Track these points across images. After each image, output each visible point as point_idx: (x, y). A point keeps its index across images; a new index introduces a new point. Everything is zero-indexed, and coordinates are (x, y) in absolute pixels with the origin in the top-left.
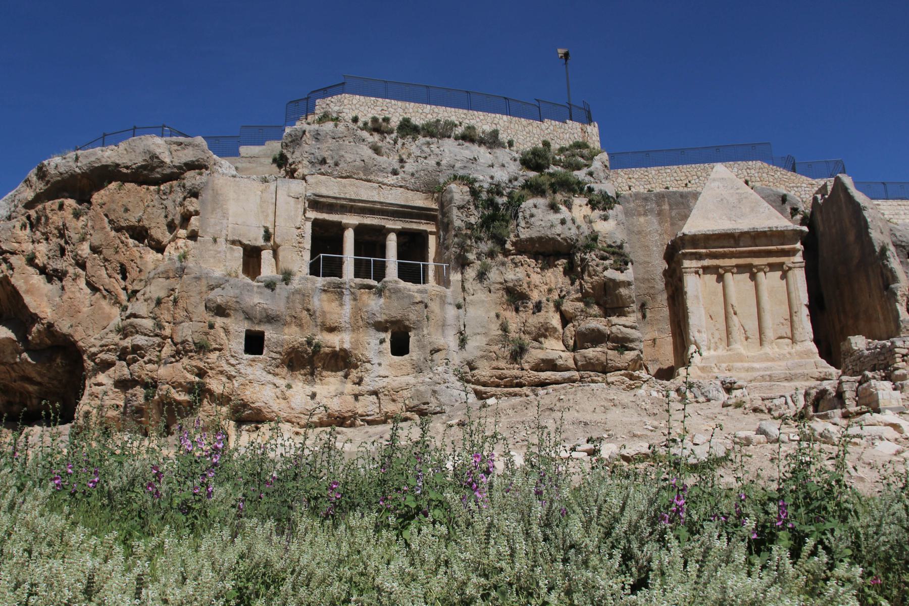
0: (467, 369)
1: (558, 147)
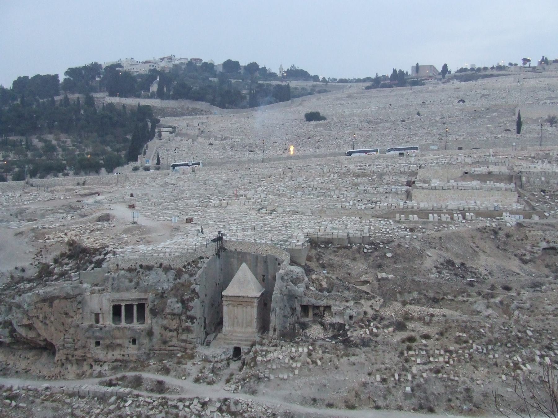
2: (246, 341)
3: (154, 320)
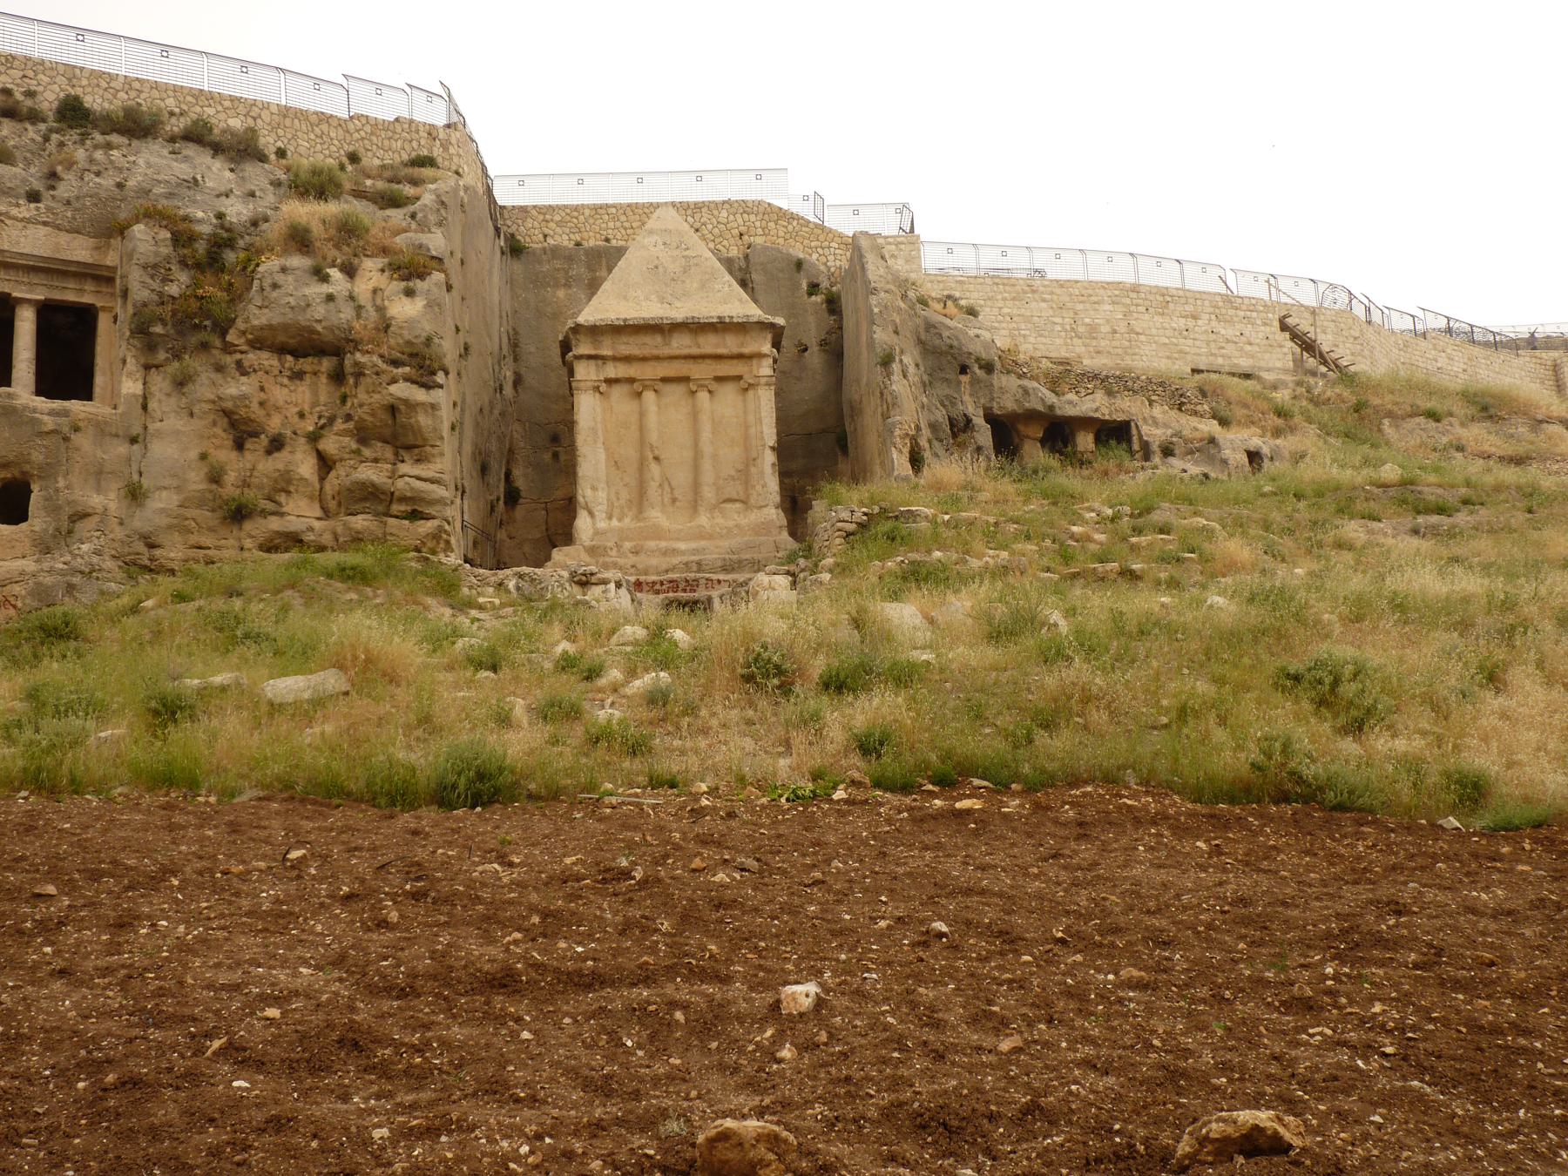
0: (142, 548)
1: (377, 162)
3: (160, 383)
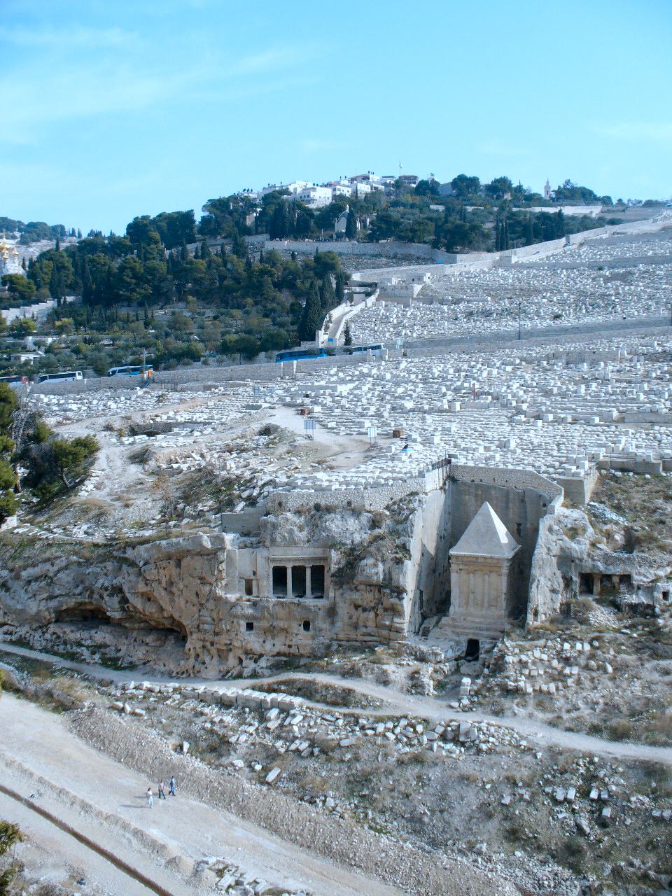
2: (488, 630)
